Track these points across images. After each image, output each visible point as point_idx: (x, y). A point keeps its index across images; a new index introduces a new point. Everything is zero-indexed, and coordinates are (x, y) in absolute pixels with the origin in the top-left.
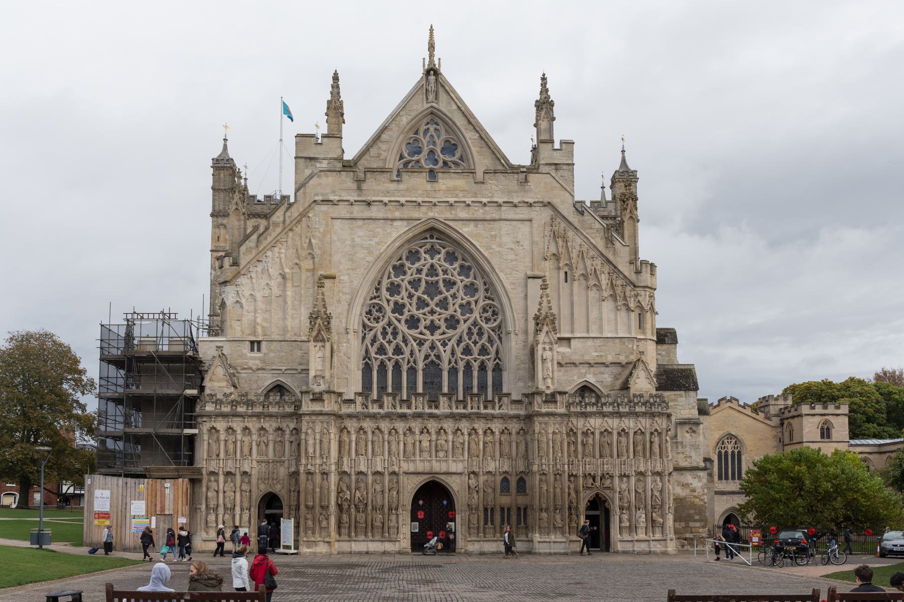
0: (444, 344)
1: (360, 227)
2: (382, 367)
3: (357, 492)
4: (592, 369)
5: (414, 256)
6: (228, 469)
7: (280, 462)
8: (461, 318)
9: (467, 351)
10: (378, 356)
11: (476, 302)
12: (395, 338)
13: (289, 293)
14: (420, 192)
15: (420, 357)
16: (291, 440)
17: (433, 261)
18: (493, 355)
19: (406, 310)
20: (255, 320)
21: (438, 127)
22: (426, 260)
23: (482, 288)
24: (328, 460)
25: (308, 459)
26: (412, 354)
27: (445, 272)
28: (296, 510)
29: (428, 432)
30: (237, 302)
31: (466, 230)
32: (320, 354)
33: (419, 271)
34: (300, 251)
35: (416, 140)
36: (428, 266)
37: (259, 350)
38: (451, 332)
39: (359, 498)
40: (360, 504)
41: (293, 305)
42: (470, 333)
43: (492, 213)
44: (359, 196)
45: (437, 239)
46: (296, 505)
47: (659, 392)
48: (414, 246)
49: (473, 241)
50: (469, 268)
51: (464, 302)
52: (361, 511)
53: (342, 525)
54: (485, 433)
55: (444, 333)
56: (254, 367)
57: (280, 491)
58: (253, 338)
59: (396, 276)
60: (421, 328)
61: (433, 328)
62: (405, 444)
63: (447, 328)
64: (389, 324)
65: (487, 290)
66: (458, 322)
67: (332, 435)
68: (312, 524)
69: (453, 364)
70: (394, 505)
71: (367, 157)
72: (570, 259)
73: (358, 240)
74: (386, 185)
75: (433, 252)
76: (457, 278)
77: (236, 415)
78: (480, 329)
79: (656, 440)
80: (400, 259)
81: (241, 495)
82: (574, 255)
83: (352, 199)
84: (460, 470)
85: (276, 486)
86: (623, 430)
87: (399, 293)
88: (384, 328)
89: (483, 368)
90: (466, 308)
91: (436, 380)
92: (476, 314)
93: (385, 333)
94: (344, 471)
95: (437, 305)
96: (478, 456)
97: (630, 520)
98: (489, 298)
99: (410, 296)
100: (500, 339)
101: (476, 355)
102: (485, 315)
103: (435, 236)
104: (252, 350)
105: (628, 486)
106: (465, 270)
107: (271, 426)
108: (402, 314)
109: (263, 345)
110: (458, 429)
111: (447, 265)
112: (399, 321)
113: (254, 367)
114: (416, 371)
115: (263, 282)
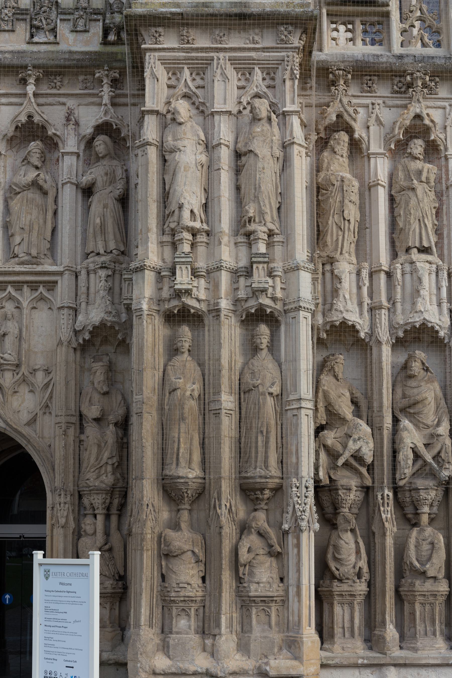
3: (405, 423)
7: (33, 285)
16: (85, 180)
24: (278, 250)
25: (174, 246)
28: (108, 516)
39: (417, 456)
40: (420, 483)
46: (111, 491)
52: (425, 519)
53: (337, 587)
57: (32, 422)
67: (295, 121)
68: (196, 581)
85: (15, 402)
94: (344, 323)
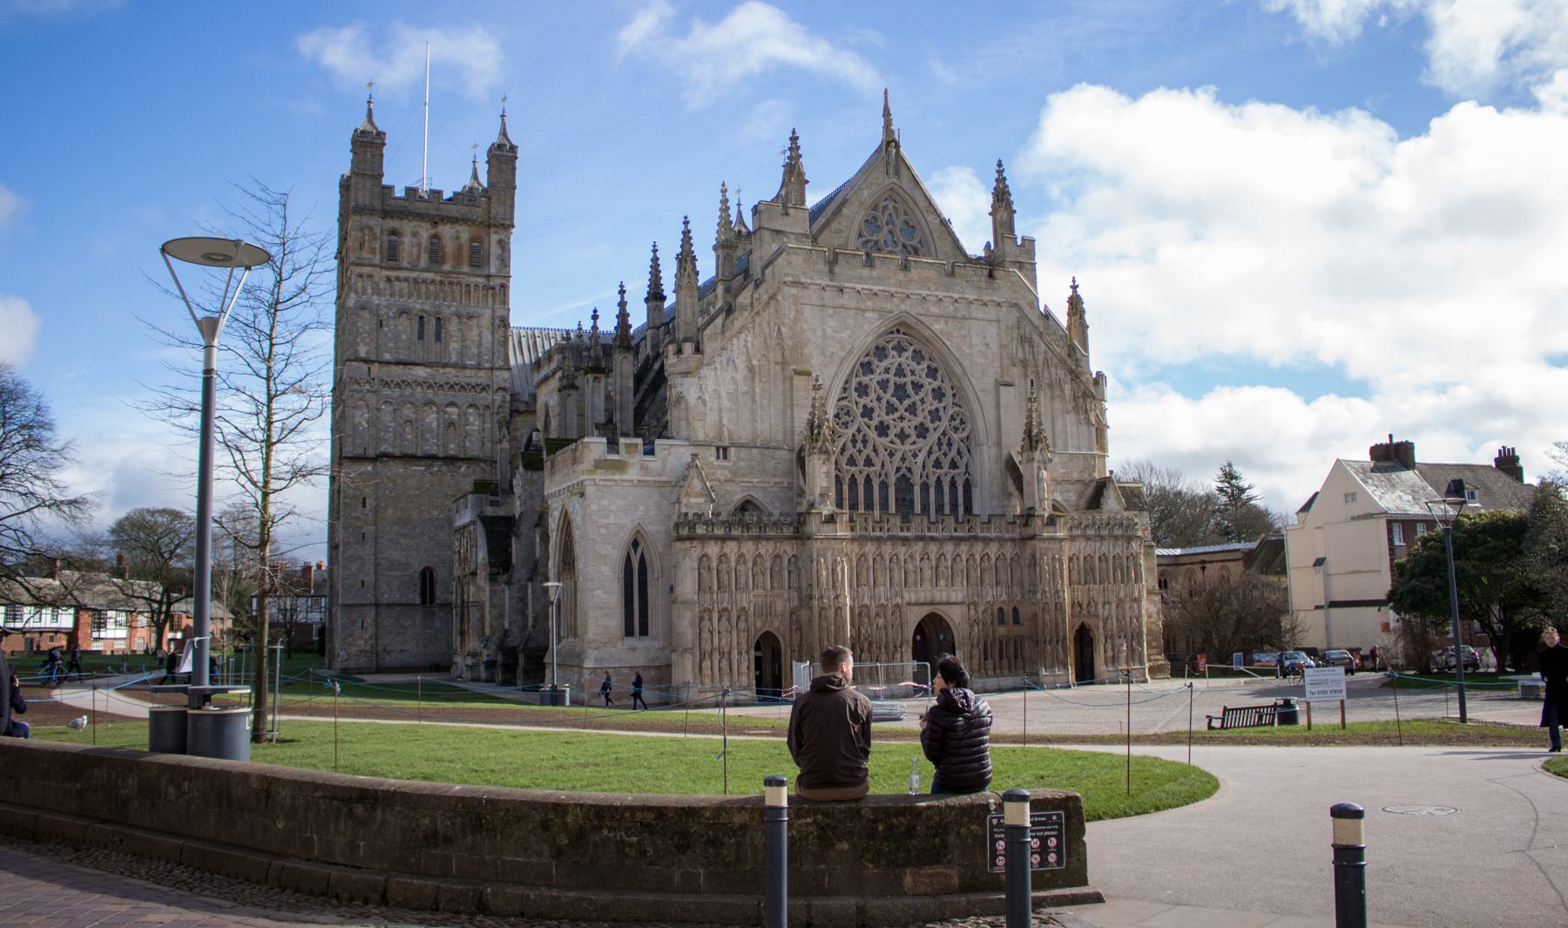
0: (915, 456)
1: (830, 316)
2: (853, 480)
4: (1058, 486)
5: (880, 352)
6: (725, 605)
8: (931, 426)
9: (938, 464)
10: (849, 467)
11: (944, 408)
12: (865, 447)
13: (758, 390)
14: (893, 281)
15: (891, 469)
17: (902, 359)
18: (962, 470)
19: (875, 415)
20: (721, 421)
21: (897, 205)
22: (893, 360)
23: (949, 393)
26: (883, 466)
27: (913, 373)
29: (928, 558)
30: (700, 398)
31: (938, 327)
32: (824, 469)
33: (887, 370)
34: (768, 341)
35: (875, 218)
36: (895, 366)
37: (725, 458)
38: (921, 442)
41: (762, 406)
42: (940, 444)
43: (962, 310)
44: (831, 280)
45: (904, 334)
47: (1130, 514)
48: (881, 342)
49: (946, 342)
50: (936, 370)
51: (933, 408)
54: (982, 559)
55: (914, 443)
56: (723, 478)
58: (719, 444)
59: (864, 374)
60: (892, 436)
61: (902, 436)
62: (905, 573)
63: (919, 436)
64: (859, 431)
65: (954, 395)
66: (927, 430)
69: (924, 478)
70: (899, 643)
71: (826, 232)
72: (1037, 366)
73: (828, 331)
74: (859, 270)
75: (900, 349)
76: (926, 381)
77: (731, 538)
78: (949, 439)
79: (1131, 565)
80: (867, 355)
81: (738, 635)
82: (1040, 363)
83: (824, 283)
84: (960, 599)
86: (1104, 555)
87: (867, 395)
88: (854, 435)
89: (953, 483)
90: (935, 415)
91: (908, 497)
92: (945, 423)
93: (854, 441)
95: (906, 410)
96: (977, 585)
97: (1113, 650)
98: (957, 405)
99: (879, 399)
100: (969, 450)
101: (946, 469)
102: (953, 423)
103: (902, 331)
104: (718, 457)
105: (1110, 614)
106: (932, 373)
107: (767, 551)
108: (871, 419)
109: (732, 452)
110: (958, 555)
111: (914, 364)
112: (869, 427)
113: (723, 478)
114: (887, 486)
115: (729, 375)
